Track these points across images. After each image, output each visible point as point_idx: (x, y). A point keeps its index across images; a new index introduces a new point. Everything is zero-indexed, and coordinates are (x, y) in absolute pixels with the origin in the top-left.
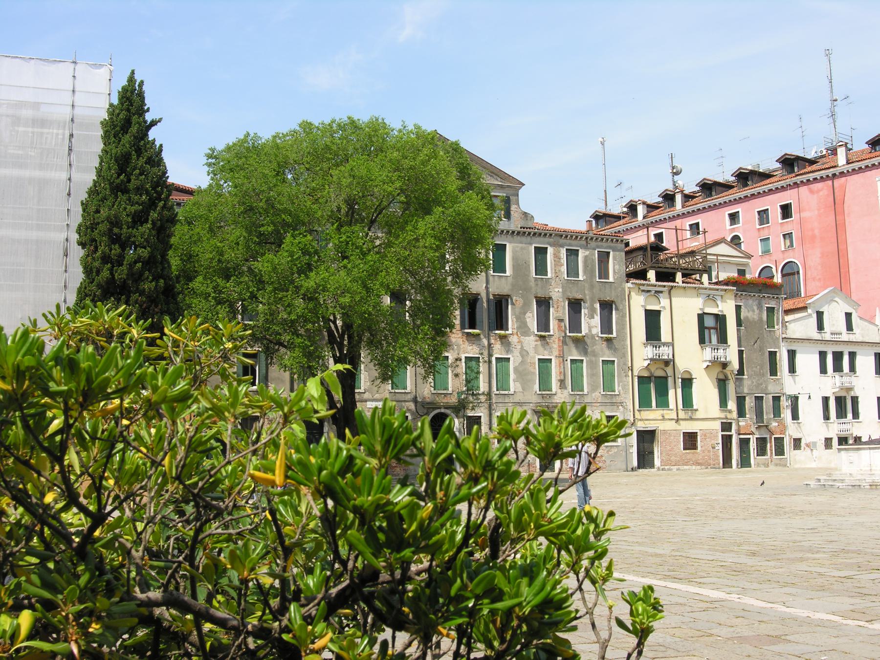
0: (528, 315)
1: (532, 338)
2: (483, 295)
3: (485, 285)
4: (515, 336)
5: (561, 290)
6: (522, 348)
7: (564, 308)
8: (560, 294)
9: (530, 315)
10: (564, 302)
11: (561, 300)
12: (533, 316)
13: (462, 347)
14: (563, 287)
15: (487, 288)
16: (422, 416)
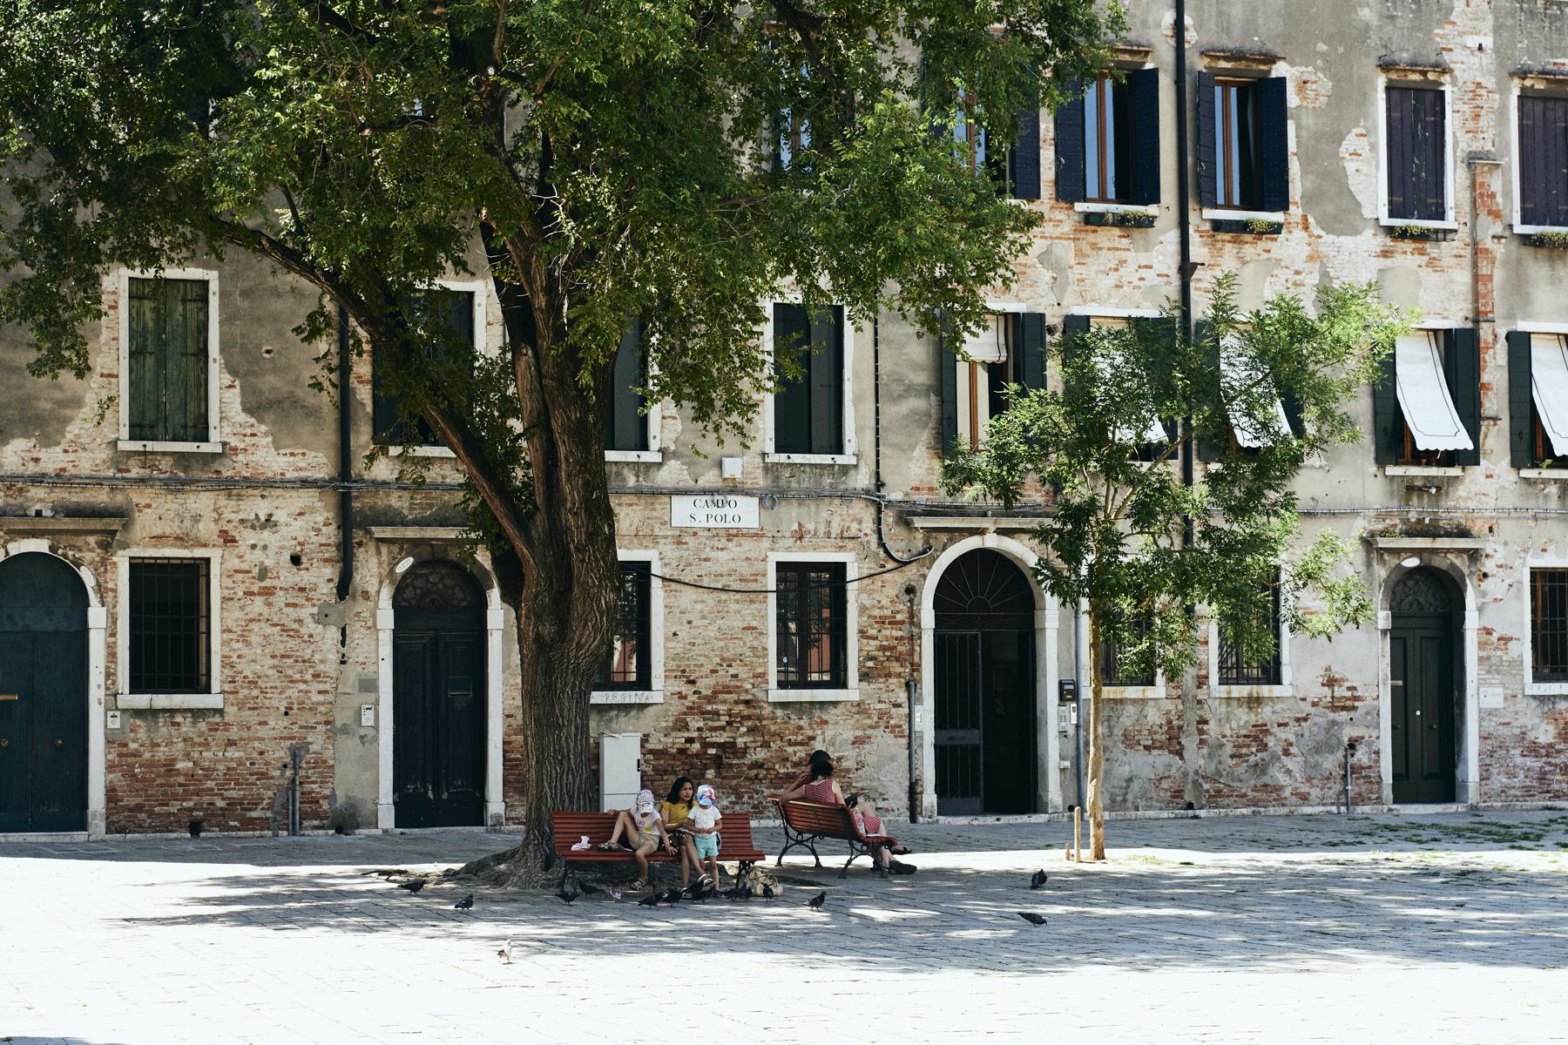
0: (1351, 143)
1: (1371, 241)
2: (1161, 59)
3: (1169, 17)
4: (1298, 234)
5: (1488, 42)
6: (1325, 275)
7: (1502, 113)
8: (1487, 59)
9: (1362, 145)
10: (1503, 90)
11: (1489, 82)
12: (1373, 147)
13: (1073, 275)
14: (1497, 29)
15: (1179, 27)
16: (903, 564)
